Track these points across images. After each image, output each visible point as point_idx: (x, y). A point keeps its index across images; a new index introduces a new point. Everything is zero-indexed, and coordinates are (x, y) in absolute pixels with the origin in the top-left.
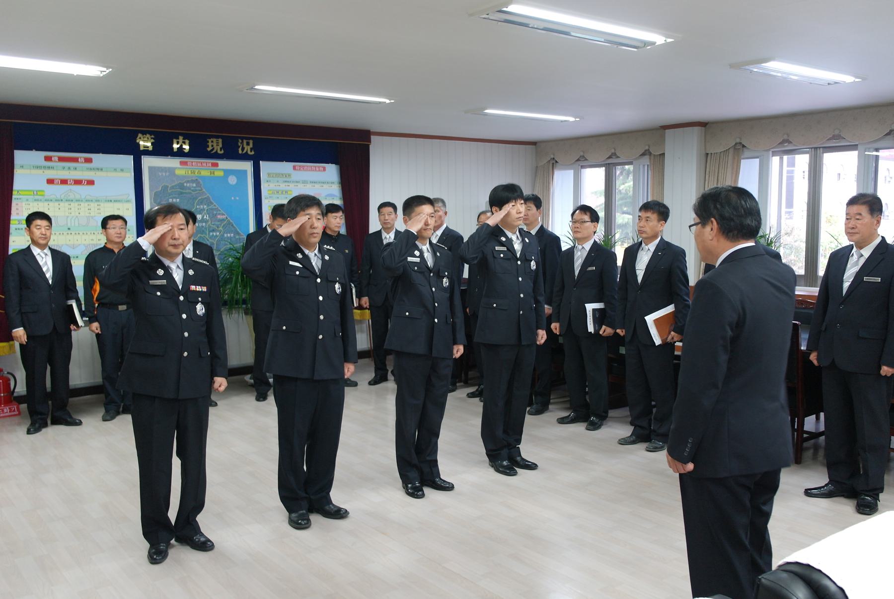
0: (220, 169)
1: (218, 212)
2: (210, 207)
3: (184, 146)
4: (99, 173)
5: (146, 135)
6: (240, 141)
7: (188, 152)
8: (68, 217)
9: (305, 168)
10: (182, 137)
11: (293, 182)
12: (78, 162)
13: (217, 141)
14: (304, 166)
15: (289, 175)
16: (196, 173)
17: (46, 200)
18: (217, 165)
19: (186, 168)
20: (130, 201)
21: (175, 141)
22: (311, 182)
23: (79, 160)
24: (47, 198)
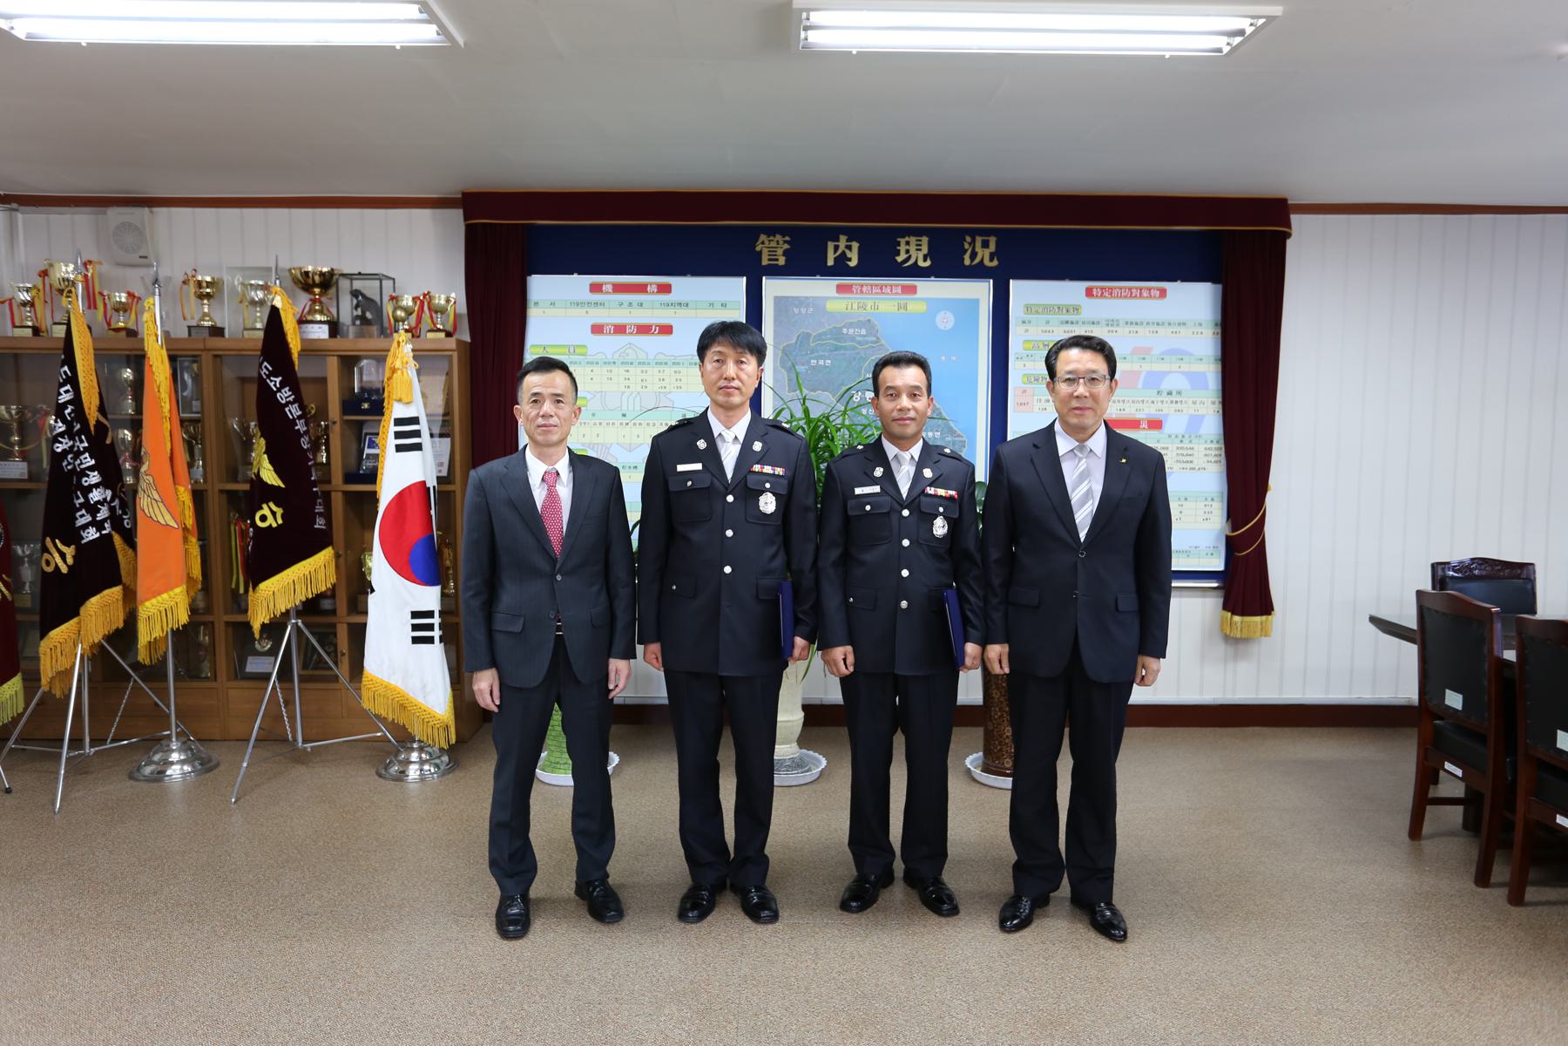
0: (916, 299)
3: (849, 255)
4: (682, 312)
5: (774, 236)
6: (968, 239)
8: (623, 393)
10: (846, 237)
11: (1083, 323)
13: (917, 240)
15: (1077, 309)
16: (868, 308)
17: (588, 363)
18: (913, 290)
19: (849, 298)
21: (831, 245)
22: (1127, 323)
24: (589, 358)
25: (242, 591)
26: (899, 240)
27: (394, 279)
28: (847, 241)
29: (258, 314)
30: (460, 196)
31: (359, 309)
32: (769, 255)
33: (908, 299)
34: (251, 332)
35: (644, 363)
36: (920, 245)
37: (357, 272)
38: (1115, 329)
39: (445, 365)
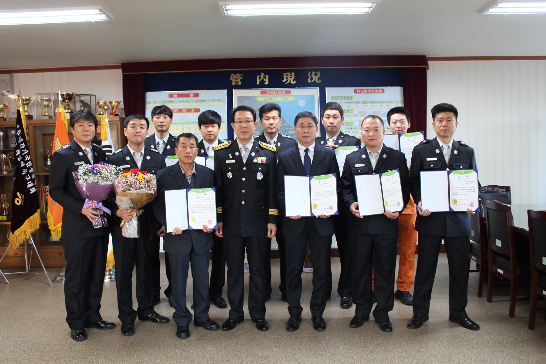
0: (292, 96)
1: (290, 128)
2: (283, 125)
3: (265, 80)
5: (237, 74)
6: (310, 73)
7: (268, 84)
9: (365, 91)
11: (354, 103)
12: (190, 96)
13: (290, 74)
14: (364, 90)
15: (351, 98)
20: (224, 122)
21: (258, 77)
22: (370, 102)
23: (190, 95)
25: (44, 212)
26: (283, 74)
27: (95, 96)
28: (264, 75)
29: (46, 110)
30: (120, 64)
31: (83, 107)
32: (235, 81)
33: (287, 96)
34: (44, 117)
35: (189, 123)
36: (291, 76)
37: (82, 94)
38: (366, 104)
39: (116, 126)
